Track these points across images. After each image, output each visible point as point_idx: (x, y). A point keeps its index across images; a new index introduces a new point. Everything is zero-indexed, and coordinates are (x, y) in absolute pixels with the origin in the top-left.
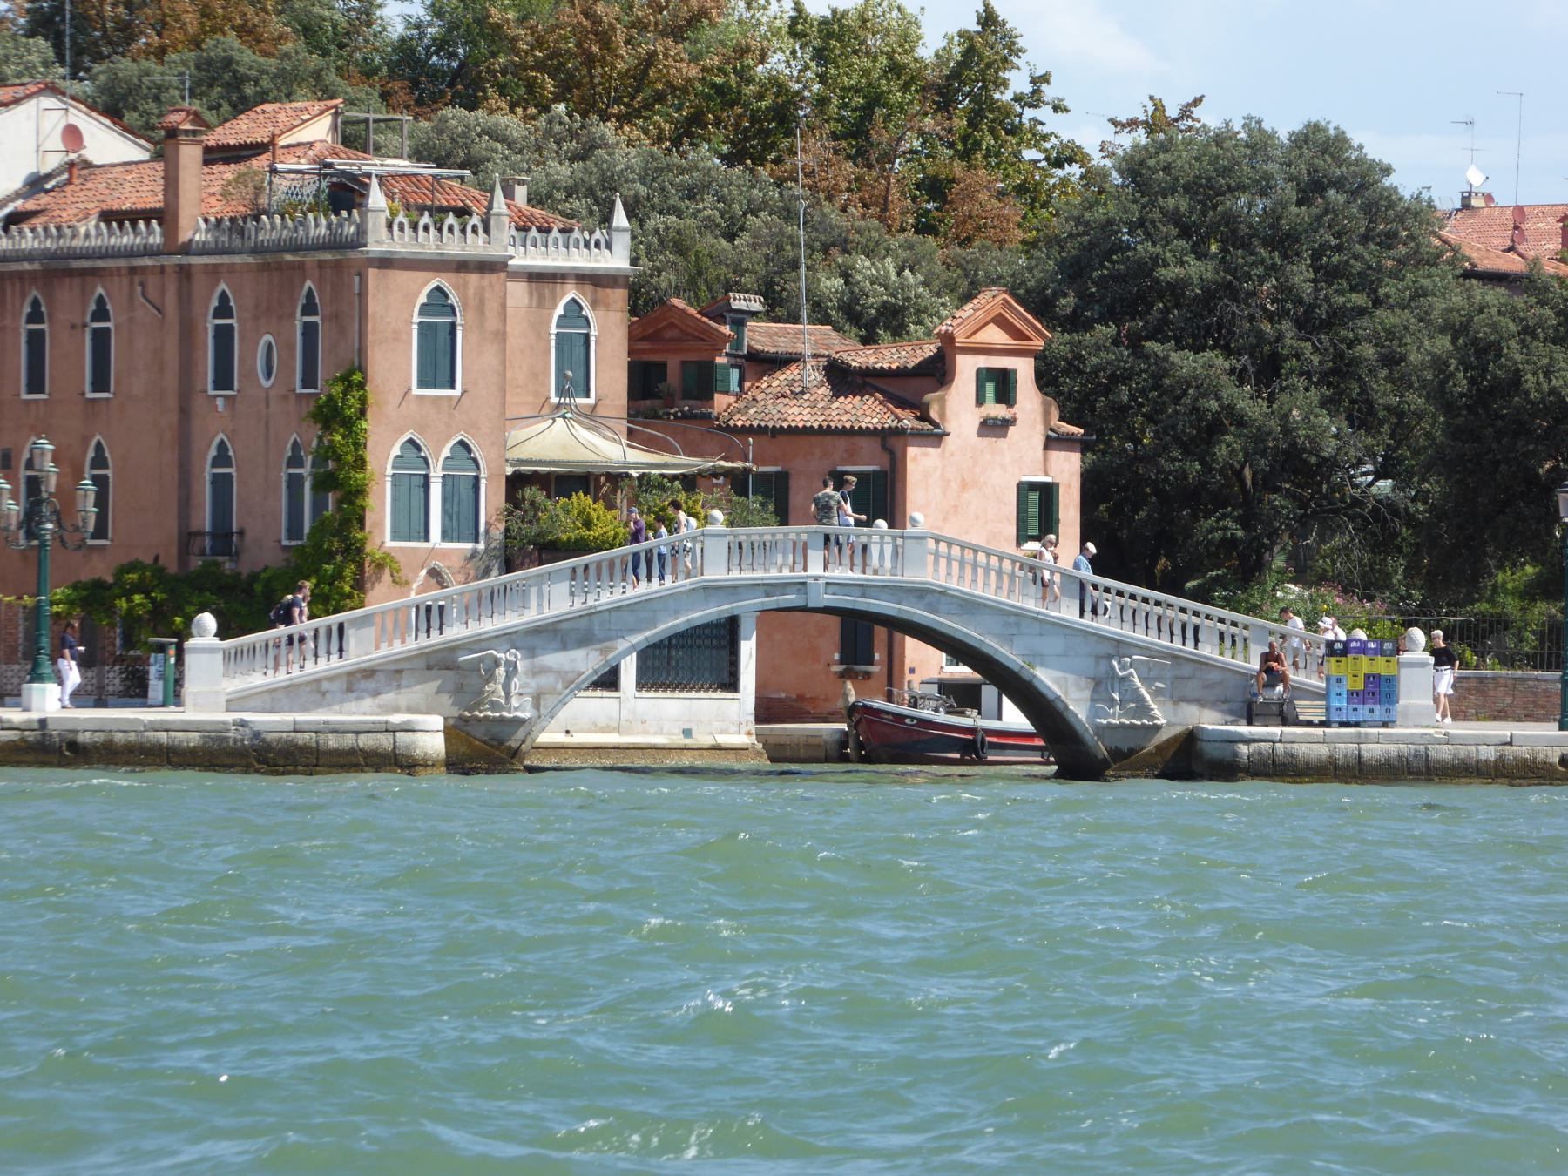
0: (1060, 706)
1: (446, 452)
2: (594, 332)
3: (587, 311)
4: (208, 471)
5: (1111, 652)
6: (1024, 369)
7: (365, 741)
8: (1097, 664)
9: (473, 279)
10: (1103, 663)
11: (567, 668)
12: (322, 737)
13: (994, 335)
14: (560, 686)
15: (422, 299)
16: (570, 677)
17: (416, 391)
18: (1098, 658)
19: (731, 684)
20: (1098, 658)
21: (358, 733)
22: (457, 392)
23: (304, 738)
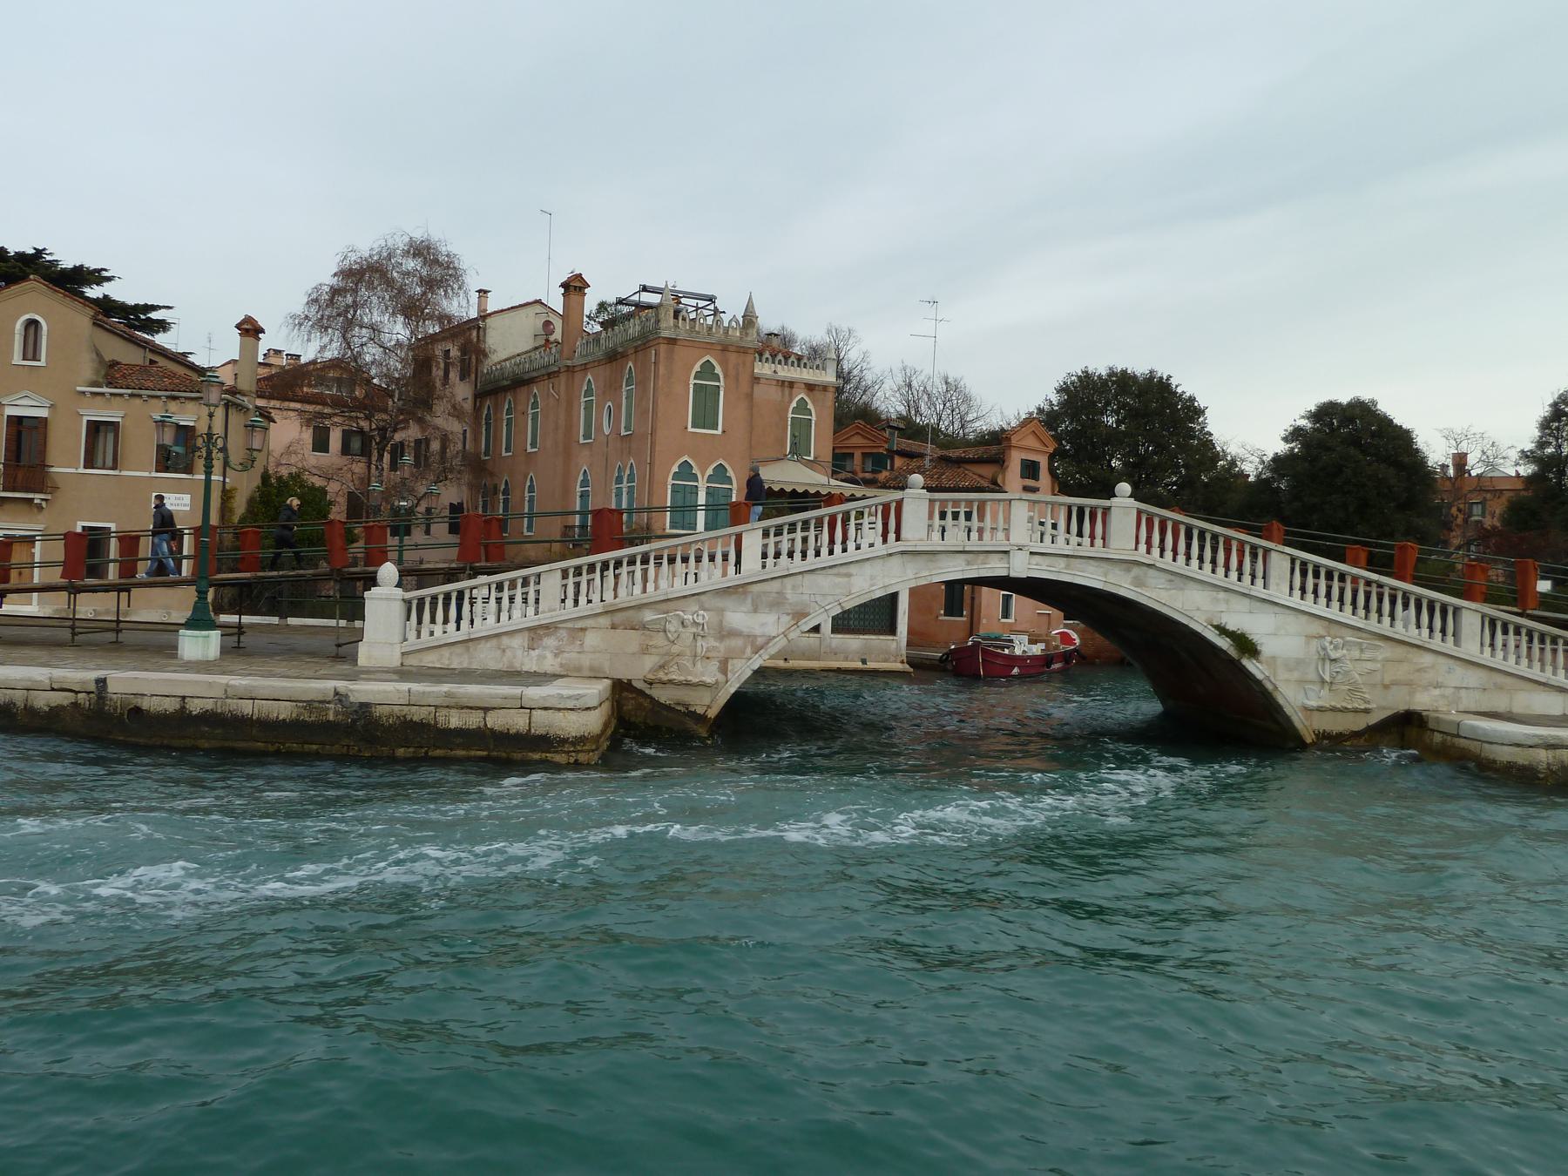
0: (1269, 687)
1: (710, 471)
2: (814, 418)
3: (810, 406)
4: (579, 489)
5: (1322, 632)
6: (1043, 461)
7: (495, 721)
8: (1307, 643)
9: (733, 358)
10: (1315, 643)
11: (758, 632)
12: (442, 712)
13: (1031, 442)
14: (749, 650)
15: (697, 368)
16: (760, 641)
17: (690, 429)
18: (1309, 637)
19: (892, 630)
20: (1309, 637)
21: (486, 710)
22: (719, 432)
23: (418, 714)
